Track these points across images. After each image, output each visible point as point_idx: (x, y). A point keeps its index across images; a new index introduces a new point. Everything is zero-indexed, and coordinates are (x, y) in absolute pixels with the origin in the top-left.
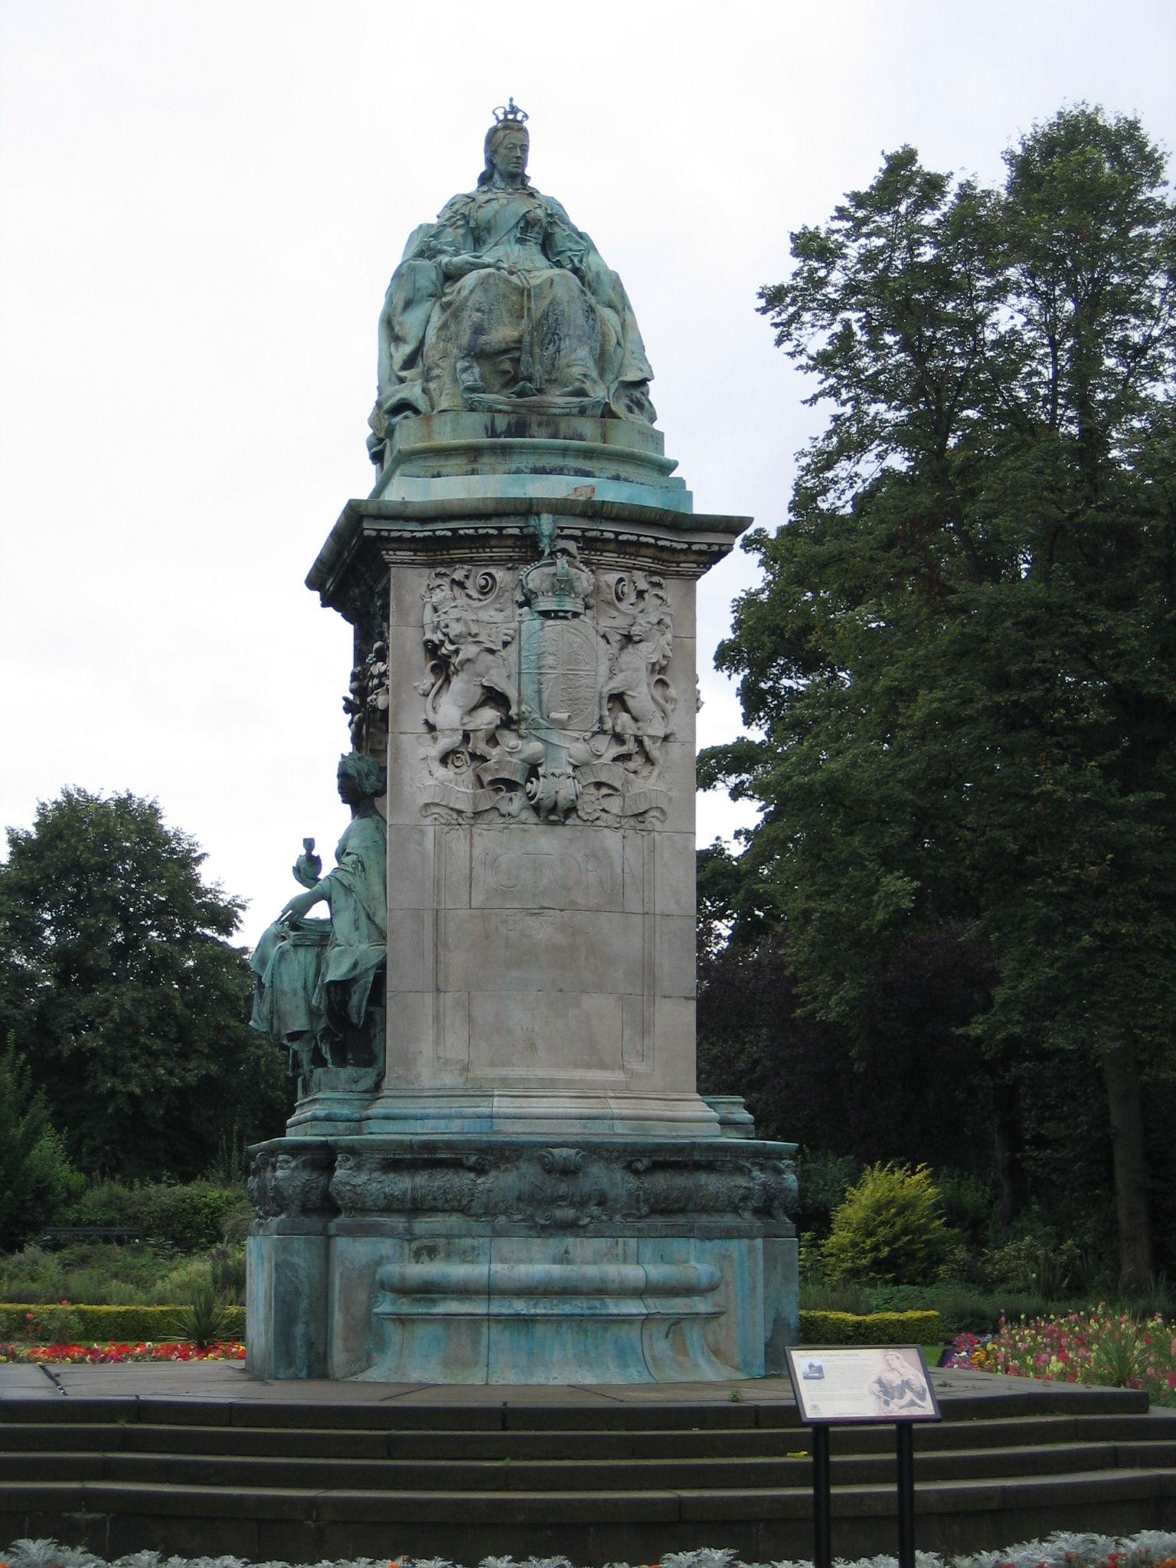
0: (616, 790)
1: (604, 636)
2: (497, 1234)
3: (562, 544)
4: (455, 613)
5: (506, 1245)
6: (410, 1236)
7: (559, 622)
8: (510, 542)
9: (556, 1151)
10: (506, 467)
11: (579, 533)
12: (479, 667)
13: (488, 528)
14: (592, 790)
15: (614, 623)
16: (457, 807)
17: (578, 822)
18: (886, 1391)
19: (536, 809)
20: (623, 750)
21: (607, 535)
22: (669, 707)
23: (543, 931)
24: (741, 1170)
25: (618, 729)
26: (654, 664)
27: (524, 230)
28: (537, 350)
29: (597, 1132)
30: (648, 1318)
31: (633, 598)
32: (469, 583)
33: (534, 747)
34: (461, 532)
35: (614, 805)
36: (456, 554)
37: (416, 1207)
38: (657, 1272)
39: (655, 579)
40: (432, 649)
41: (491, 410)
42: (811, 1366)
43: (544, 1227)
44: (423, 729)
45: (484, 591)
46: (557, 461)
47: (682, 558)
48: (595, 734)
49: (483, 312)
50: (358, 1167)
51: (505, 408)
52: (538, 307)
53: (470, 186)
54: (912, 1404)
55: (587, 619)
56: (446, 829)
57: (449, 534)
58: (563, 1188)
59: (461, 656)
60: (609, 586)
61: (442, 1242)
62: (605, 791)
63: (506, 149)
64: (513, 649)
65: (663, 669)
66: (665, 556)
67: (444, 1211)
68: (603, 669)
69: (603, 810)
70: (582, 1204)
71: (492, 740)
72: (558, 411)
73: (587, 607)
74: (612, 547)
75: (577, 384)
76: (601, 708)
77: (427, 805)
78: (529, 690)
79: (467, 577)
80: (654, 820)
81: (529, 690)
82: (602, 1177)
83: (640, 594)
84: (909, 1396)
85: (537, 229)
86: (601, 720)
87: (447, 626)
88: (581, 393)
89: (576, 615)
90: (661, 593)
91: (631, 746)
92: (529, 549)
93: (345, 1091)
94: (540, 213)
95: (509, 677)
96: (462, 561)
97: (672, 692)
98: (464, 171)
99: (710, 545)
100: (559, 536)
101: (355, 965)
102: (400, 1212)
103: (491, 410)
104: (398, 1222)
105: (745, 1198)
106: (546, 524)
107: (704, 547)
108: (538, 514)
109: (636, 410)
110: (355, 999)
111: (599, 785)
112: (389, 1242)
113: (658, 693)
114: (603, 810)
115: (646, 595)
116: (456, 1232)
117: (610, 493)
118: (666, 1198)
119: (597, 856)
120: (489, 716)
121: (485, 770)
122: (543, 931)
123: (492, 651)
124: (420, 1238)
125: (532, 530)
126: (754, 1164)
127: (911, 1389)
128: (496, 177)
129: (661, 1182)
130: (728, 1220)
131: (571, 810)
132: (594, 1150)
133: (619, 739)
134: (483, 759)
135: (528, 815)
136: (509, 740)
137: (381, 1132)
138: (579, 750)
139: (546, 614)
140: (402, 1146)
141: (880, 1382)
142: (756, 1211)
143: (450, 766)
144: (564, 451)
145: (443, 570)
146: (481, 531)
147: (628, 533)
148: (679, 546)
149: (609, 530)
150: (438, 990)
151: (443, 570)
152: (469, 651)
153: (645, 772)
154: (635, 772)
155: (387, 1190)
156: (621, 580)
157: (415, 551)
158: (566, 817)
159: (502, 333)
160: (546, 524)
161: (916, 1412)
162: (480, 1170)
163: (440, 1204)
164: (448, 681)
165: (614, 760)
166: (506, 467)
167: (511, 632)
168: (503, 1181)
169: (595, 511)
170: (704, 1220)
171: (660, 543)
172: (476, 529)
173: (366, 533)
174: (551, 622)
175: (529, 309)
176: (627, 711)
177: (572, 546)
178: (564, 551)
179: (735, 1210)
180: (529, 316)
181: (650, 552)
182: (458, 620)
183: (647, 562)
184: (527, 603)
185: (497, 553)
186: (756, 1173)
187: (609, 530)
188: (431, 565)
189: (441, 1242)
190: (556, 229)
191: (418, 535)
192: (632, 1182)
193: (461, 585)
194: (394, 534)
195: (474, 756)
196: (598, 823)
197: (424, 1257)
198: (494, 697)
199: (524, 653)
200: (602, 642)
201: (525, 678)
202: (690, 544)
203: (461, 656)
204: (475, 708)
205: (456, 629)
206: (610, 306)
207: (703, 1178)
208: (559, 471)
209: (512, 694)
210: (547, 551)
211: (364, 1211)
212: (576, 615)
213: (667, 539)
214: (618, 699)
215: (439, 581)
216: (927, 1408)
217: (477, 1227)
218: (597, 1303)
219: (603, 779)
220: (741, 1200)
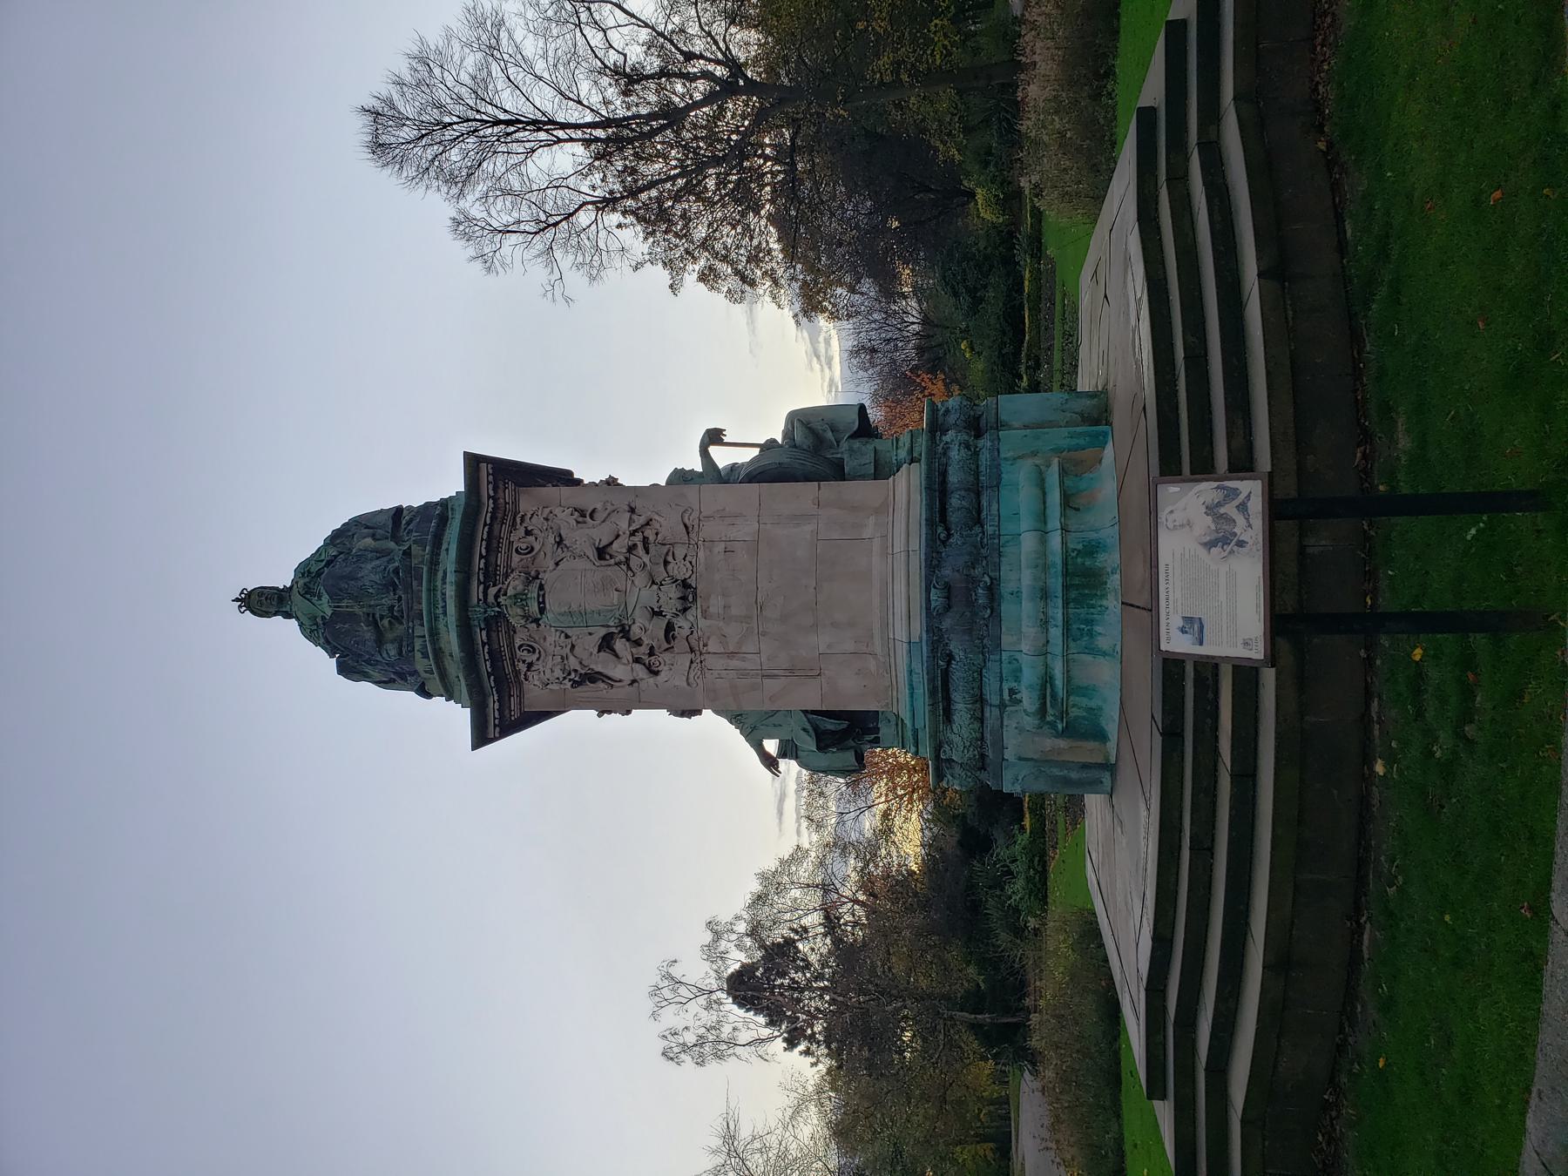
3: (491, 599)
4: (548, 671)
6: (1002, 706)
9: (933, 604)
14: (670, 567)
18: (1222, 540)
19: (685, 610)
20: (640, 545)
22: (610, 508)
29: (917, 562)
30: (1065, 529)
31: (531, 538)
32: (529, 660)
35: (680, 552)
37: (980, 700)
38: (1026, 523)
40: (576, 684)
42: (1183, 631)
48: (629, 568)
50: (950, 743)
54: (1242, 508)
55: (546, 577)
62: (670, 558)
64: (569, 632)
66: (500, 516)
68: (581, 564)
70: (973, 582)
71: (638, 643)
83: (528, 533)
84: (1230, 509)
88: (396, 571)
89: (541, 587)
91: (638, 539)
92: (496, 622)
94: (301, 582)
96: (513, 664)
97: (599, 506)
104: (991, 714)
105: (968, 447)
111: (666, 563)
113: (600, 516)
118: (970, 512)
120: (620, 645)
123: (573, 646)
127: (1219, 505)
130: (985, 458)
131: (685, 584)
133: (632, 548)
134: (652, 648)
135: (690, 615)
136: (636, 631)
137: (924, 719)
138: (641, 579)
139: (542, 610)
140: (933, 712)
141: (1209, 545)
142: (978, 436)
147: (480, 548)
149: (478, 564)
152: (573, 663)
158: (690, 586)
161: (1256, 505)
163: (976, 685)
177: (493, 591)
179: (976, 454)
181: (496, 527)
184: (536, 621)
185: (503, 642)
186: (947, 438)
187: (478, 564)
193: (530, 665)
195: (651, 654)
198: (606, 644)
200: (561, 565)
204: (617, 656)
205: (558, 673)
209: (603, 632)
211: (982, 739)
214: (602, 553)
216: (1251, 490)
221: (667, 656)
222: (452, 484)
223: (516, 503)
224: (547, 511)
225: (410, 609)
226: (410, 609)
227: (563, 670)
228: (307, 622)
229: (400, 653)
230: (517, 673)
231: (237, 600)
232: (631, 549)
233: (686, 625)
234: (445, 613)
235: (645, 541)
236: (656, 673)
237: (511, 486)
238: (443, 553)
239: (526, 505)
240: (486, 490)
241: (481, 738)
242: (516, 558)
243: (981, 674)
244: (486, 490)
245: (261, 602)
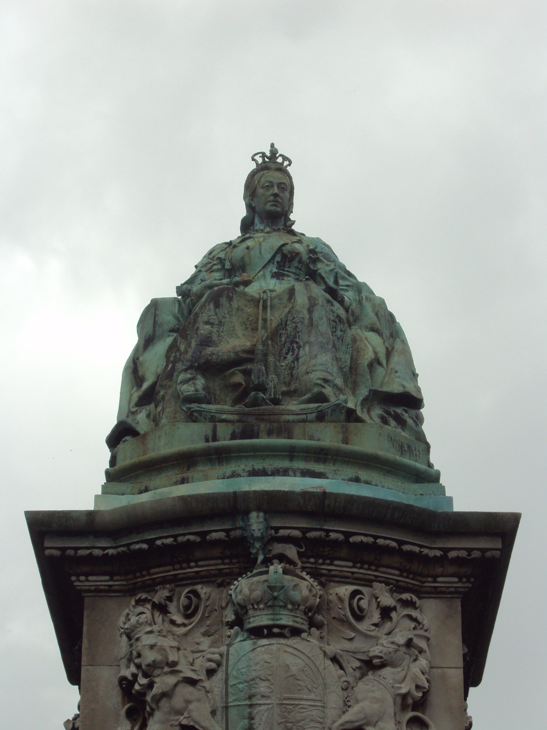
1: (335, 660)
4: (148, 640)
7: (273, 641)
8: (217, 552)
11: (297, 533)
12: (177, 701)
13: (188, 535)
15: (347, 646)
21: (333, 535)
26: (404, 697)
27: (280, 266)
28: (271, 359)
31: (376, 617)
32: (172, 607)
34: (159, 542)
36: (158, 573)
39: (406, 596)
40: (126, 685)
41: (213, 419)
45: (189, 613)
46: (286, 464)
47: (439, 570)
49: (212, 324)
52: (274, 318)
53: (234, 233)
57: (145, 546)
59: (156, 690)
60: (341, 600)
63: (269, 193)
64: (220, 675)
65: (421, 704)
68: (334, 699)
72: (291, 418)
73: (312, 624)
74: (344, 553)
75: (316, 390)
79: (170, 599)
83: (386, 613)
85: (295, 263)
87: (139, 655)
88: (321, 398)
89: (296, 632)
90: (414, 613)
92: (240, 557)
95: (213, 713)
96: (164, 581)
98: (224, 220)
99: (470, 550)
103: (213, 419)
106: (256, 523)
107: (463, 554)
108: (247, 513)
109: (393, 423)
115: (393, 615)
117: (335, 483)
123: (193, 682)
125: (238, 533)
128: (257, 220)
139: (257, 633)
144: (292, 453)
145: (144, 596)
146: (180, 539)
148: (432, 553)
149: (336, 530)
151: (144, 596)
152: (164, 682)
156: (354, 594)
157: (112, 574)
159: (233, 341)
167: (217, 657)
169: (321, 507)
171: (406, 548)
172: (175, 537)
173: (47, 552)
174: (264, 641)
175: (265, 320)
177: (291, 552)
178: (282, 558)
180: (264, 327)
182: (152, 647)
183: (394, 575)
187: (336, 530)
188: (131, 591)
190: (319, 265)
191: (111, 552)
193: (162, 609)
194: (81, 552)
199: (231, 682)
200: (332, 668)
201: (233, 713)
202: (446, 550)
203: (156, 690)
205: (150, 657)
206: (373, 329)
208: (285, 472)
210: (261, 558)
215: (140, 609)
222: (466, 491)
223: (436, 593)
224: (423, 644)
225: (260, 417)
226: (260, 417)
227: (154, 665)
228: (239, 252)
229: (189, 400)
230: (151, 587)
231: (274, 152)
234: (254, 473)
238: (350, 472)
239: (430, 612)
240: (459, 547)
241: (45, 528)
244: (459, 547)
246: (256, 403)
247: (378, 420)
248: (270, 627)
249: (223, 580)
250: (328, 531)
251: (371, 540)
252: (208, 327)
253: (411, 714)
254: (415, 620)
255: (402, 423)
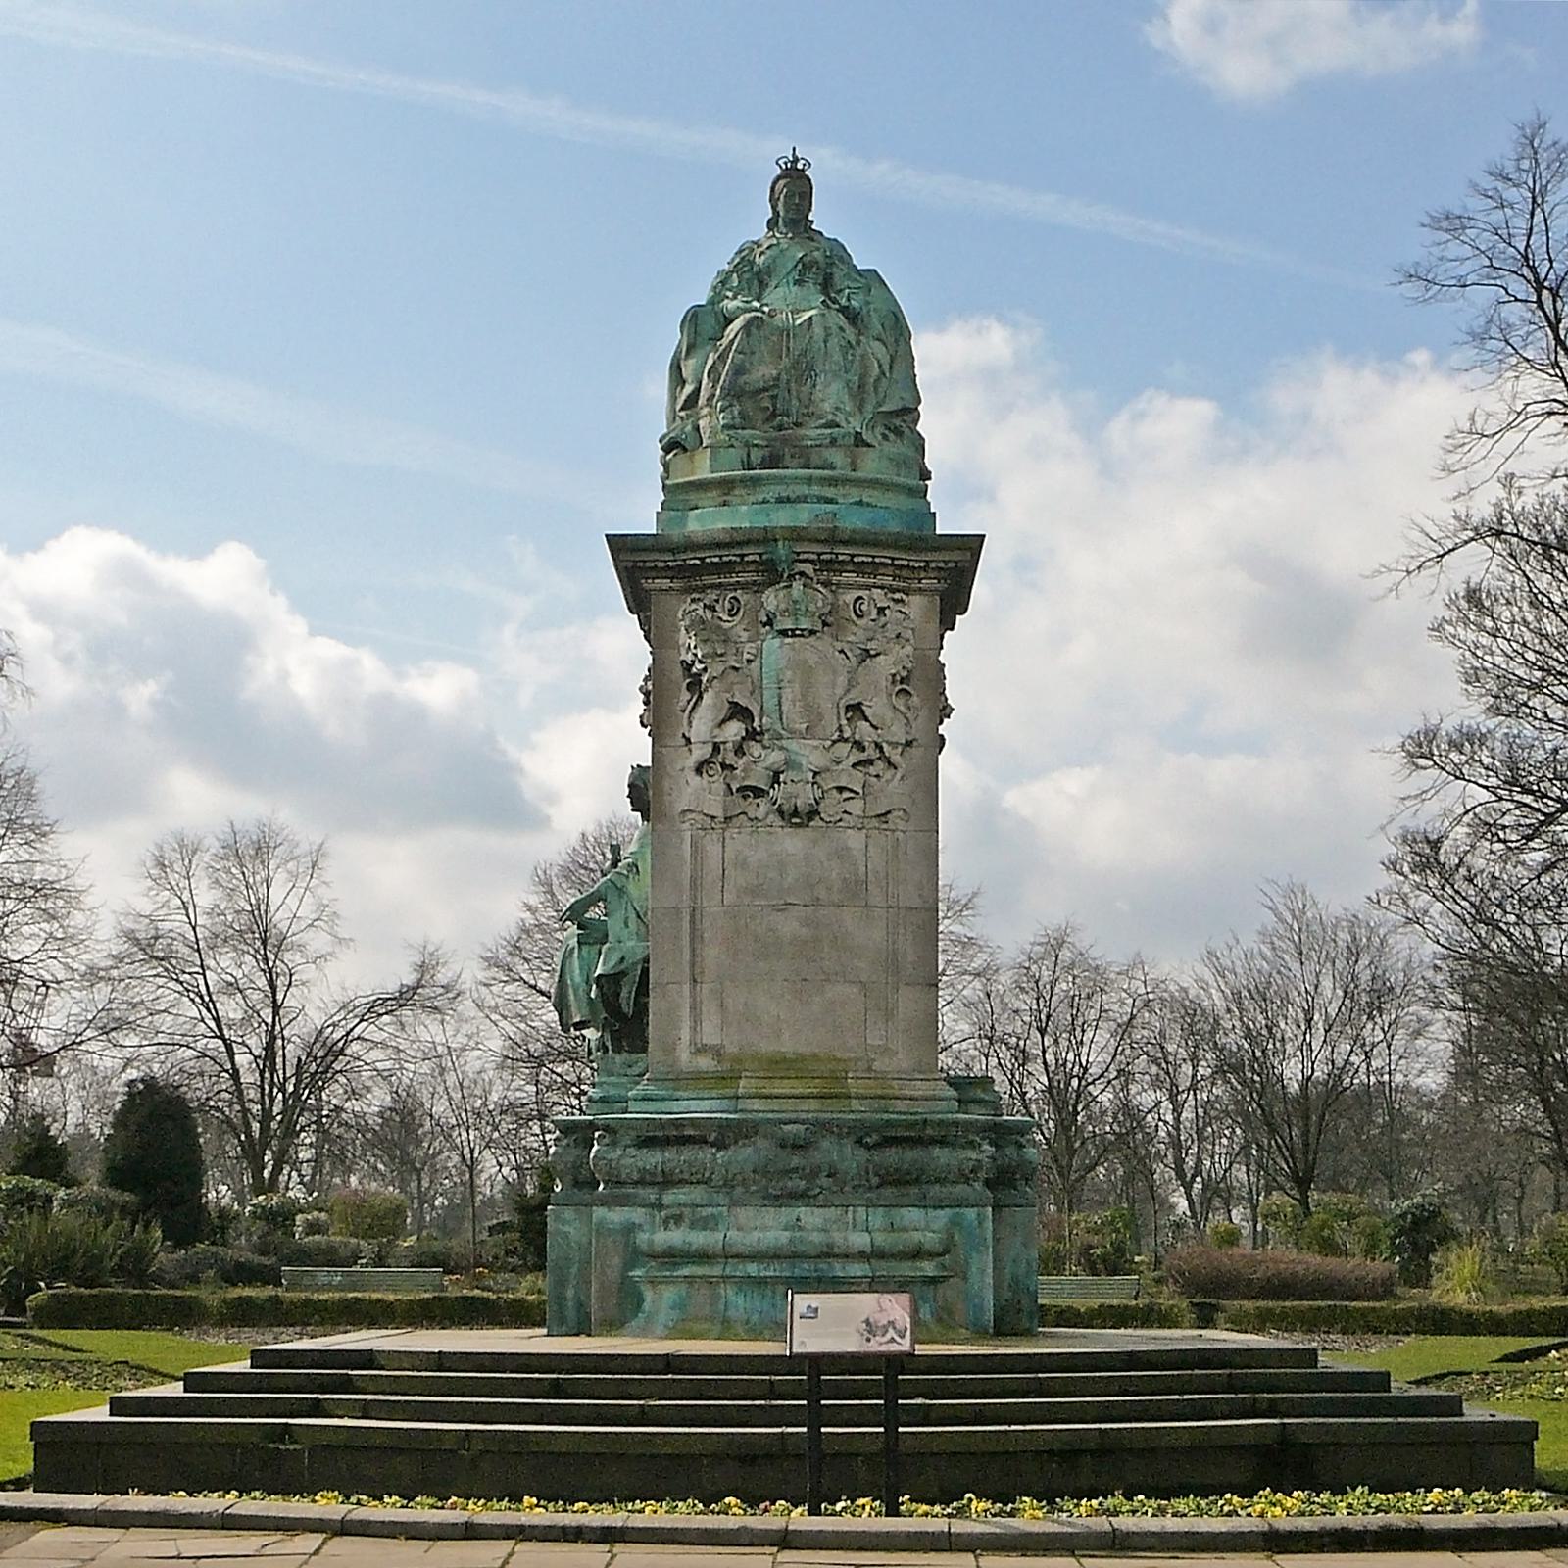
0: (858, 793)
2: (734, 1203)
5: (744, 1214)
7: (796, 639)
8: (752, 568)
10: (752, 499)
11: (815, 557)
16: (711, 813)
17: (821, 823)
18: (871, 1329)
19: (780, 812)
20: (863, 756)
21: (841, 557)
23: (789, 926)
24: (972, 1145)
25: (857, 737)
26: (894, 676)
33: (775, 758)
34: (708, 560)
35: (856, 807)
37: (667, 1180)
39: (897, 596)
42: (809, 1307)
43: (777, 1197)
44: (683, 741)
46: (805, 490)
49: (745, 354)
50: (614, 1144)
51: (761, 443)
54: (892, 1340)
56: (701, 833)
58: (795, 1161)
61: (687, 1211)
62: (846, 794)
64: (755, 665)
66: (904, 573)
67: (692, 1183)
69: (845, 812)
71: (739, 751)
75: (830, 417)
76: (839, 719)
77: (684, 812)
78: (770, 703)
79: (717, 601)
80: (898, 821)
81: (770, 703)
82: (829, 1151)
83: (881, 610)
84: (891, 1333)
85: (814, 270)
86: (840, 729)
89: (812, 632)
91: (871, 752)
92: (772, 574)
93: (620, 1075)
96: (713, 586)
98: (753, 222)
100: (796, 561)
101: (623, 959)
102: (653, 1184)
103: (747, 445)
104: (651, 1194)
106: (782, 550)
109: (892, 436)
110: (624, 994)
111: (840, 789)
112: (641, 1211)
114: (845, 812)
115: (887, 611)
116: (698, 1201)
119: (842, 854)
120: (735, 730)
121: (734, 778)
122: (789, 926)
124: (668, 1207)
126: (983, 1139)
127: (894, 1328)
129: (891, 1156)
130: (961, 1189)
131: (813, 814)
132: (823, 1127)
133: (859, 745)
135: (774, 818)
136: (755, 749)
139: (783, 633)
141: (867, 1322)
142: (987, 1183)
143: (704, 775)
146: (725, 559)
147: (863, 555)
150: (695, 981)
153: (888, 775)
154: (877, 776)
155: (640, 1164)
158: (810, 819)
159: (762, 372)
160: (782, 550)
161: (894, 1348)
162: (721, 1145)
163: (686, 1176)
164: (700, 697)
165: (854, 766)
166: (752, 499)
167: (754, 651)
168: (743, 1155)
170: (935, 1190)
172: (721, 556)
174: (789, 640)
176: (867, 720)
177: (808, 568)
179: (967, 1181)
181: (890, 571)
183: (888, 581)
184: (770, 623)
189: (687, 1211)
192: (862, 1154)
195: (724, 766)
196: (840, 824)
197: (672, 1225)
198: (738, 712)
204: (724, 722)
207: (936, 1151)
208: (804, 499)
212: (812, 632)
213: (903, 558)
215: (694, 606)
217: (721, 1199)
218: (824, 1266)
219: (843, 784)
220: (972, 1172)
221: (719, 786)
225: (785, 441)
230: (703, 589)
231: (796, 160)
232: (859, 745)
233: (761, 813)
235: (871, 762)
236: (698, 771)
237: (943, 586)
240: (937, 558)
241: (620, 546)
242: (849, 597)
243: (698, 1183)
245: (794, 189)
246: (780, 428)
247: (880, 437)
248: (793, 630)
249: (758, 588)
250: (837, 554)
251: (870, 559)
252: (741, 356)
253: (899, 687)
254: (904, 613)
255: (898, 433)
